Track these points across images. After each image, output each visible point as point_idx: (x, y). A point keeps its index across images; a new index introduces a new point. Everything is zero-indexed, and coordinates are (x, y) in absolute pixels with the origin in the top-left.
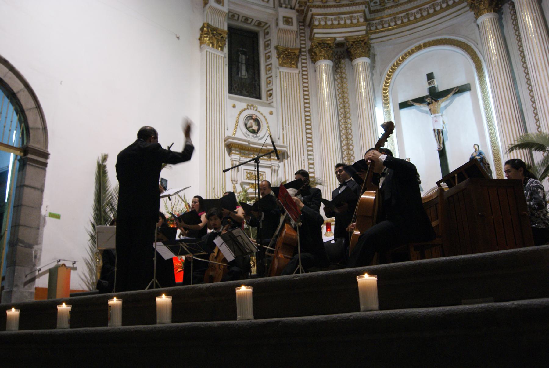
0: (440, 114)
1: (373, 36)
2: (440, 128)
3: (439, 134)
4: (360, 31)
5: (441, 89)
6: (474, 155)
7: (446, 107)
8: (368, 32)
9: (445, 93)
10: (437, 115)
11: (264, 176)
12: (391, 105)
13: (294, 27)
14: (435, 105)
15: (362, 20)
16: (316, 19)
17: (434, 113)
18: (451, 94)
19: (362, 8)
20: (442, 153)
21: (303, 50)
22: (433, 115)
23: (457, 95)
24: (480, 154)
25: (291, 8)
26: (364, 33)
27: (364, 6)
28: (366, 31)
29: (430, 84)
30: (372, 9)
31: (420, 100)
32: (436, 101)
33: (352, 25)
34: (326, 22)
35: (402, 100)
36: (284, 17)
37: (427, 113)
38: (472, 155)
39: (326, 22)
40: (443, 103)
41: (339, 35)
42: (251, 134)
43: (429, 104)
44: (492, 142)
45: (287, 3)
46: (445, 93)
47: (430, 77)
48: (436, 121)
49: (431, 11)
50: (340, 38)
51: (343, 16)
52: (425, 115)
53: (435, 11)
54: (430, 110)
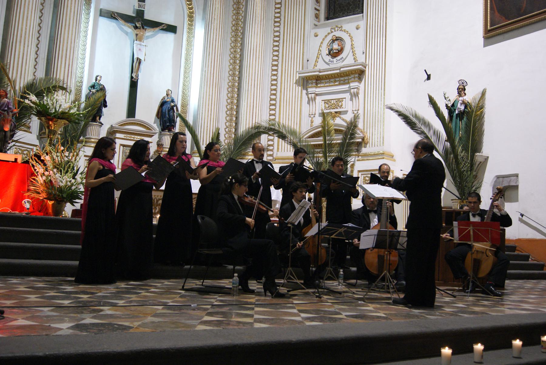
0: (144, 44)
2: (142, 59)
3: (136, 64)
5: (147, 16)
6: (166, 99)
7: (148, 37)
9: (154, 25)
10: (142, 44)
12: (93, 5)
14: (140, 32)
17: (140, 41)
18: (157, 29)
20: (134, 85)
22: (138, 42)
23: (162, 31)
24: (173, 101)
29: (140, 6)
31: (127, 19)
32: (143, 28)
35: (105, 5)
37: (127, 33)
38: (164, 98)
40: (149, 32)
43: (136, 28)
44: (183, 93)
46: (154, 25)
48: (140, 50)
52: (124, 35)
54: (137, 35)
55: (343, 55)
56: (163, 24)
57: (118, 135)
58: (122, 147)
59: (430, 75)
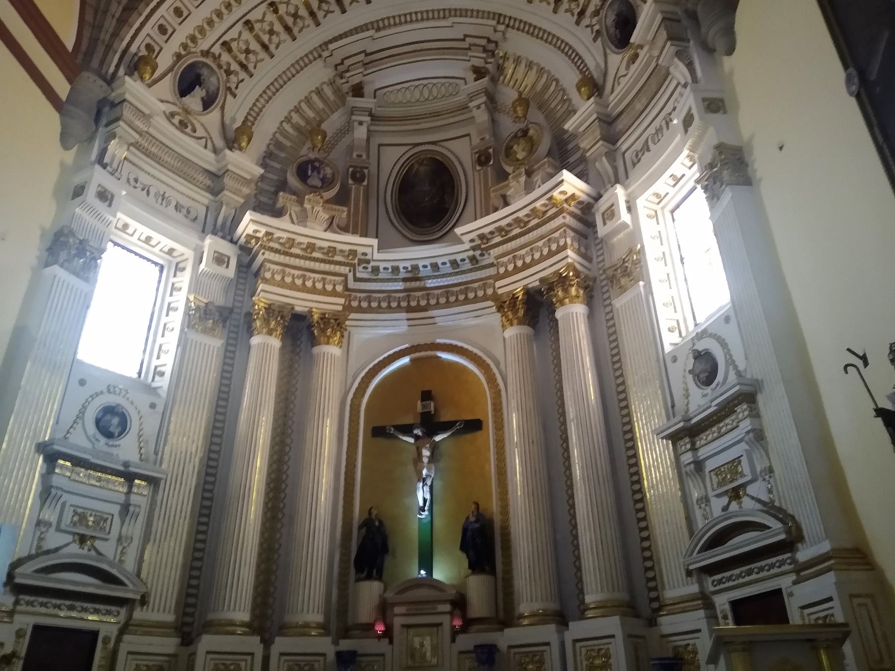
1: (353, 316)
4: (335, 304)
8: (348, 308)
11: (109, 521)
13: (231, 272)
15: (339, 288)
16: (269, 269)
19: (344, 270)
21: (235, 310)
25: (231, 241)
26: (340, 308)
27: (348, 268)
28: (344, 306)
29: (424, 407)
30: (358, 275)
33: (324, 292)
34: (283, 278)
36: (215, 252)
39: (283, 278)
41: (302, 302)
42: (103, 440)
45: (227, 231)
47: (427, 396)
49: (443, 300)
50: (300, 307)
51: (313, 275)
53: (448, 301)
55: (720, 377)
56: (457, 422)
57: (398, 610)
58: (405, 629)
59: (865, 355)
